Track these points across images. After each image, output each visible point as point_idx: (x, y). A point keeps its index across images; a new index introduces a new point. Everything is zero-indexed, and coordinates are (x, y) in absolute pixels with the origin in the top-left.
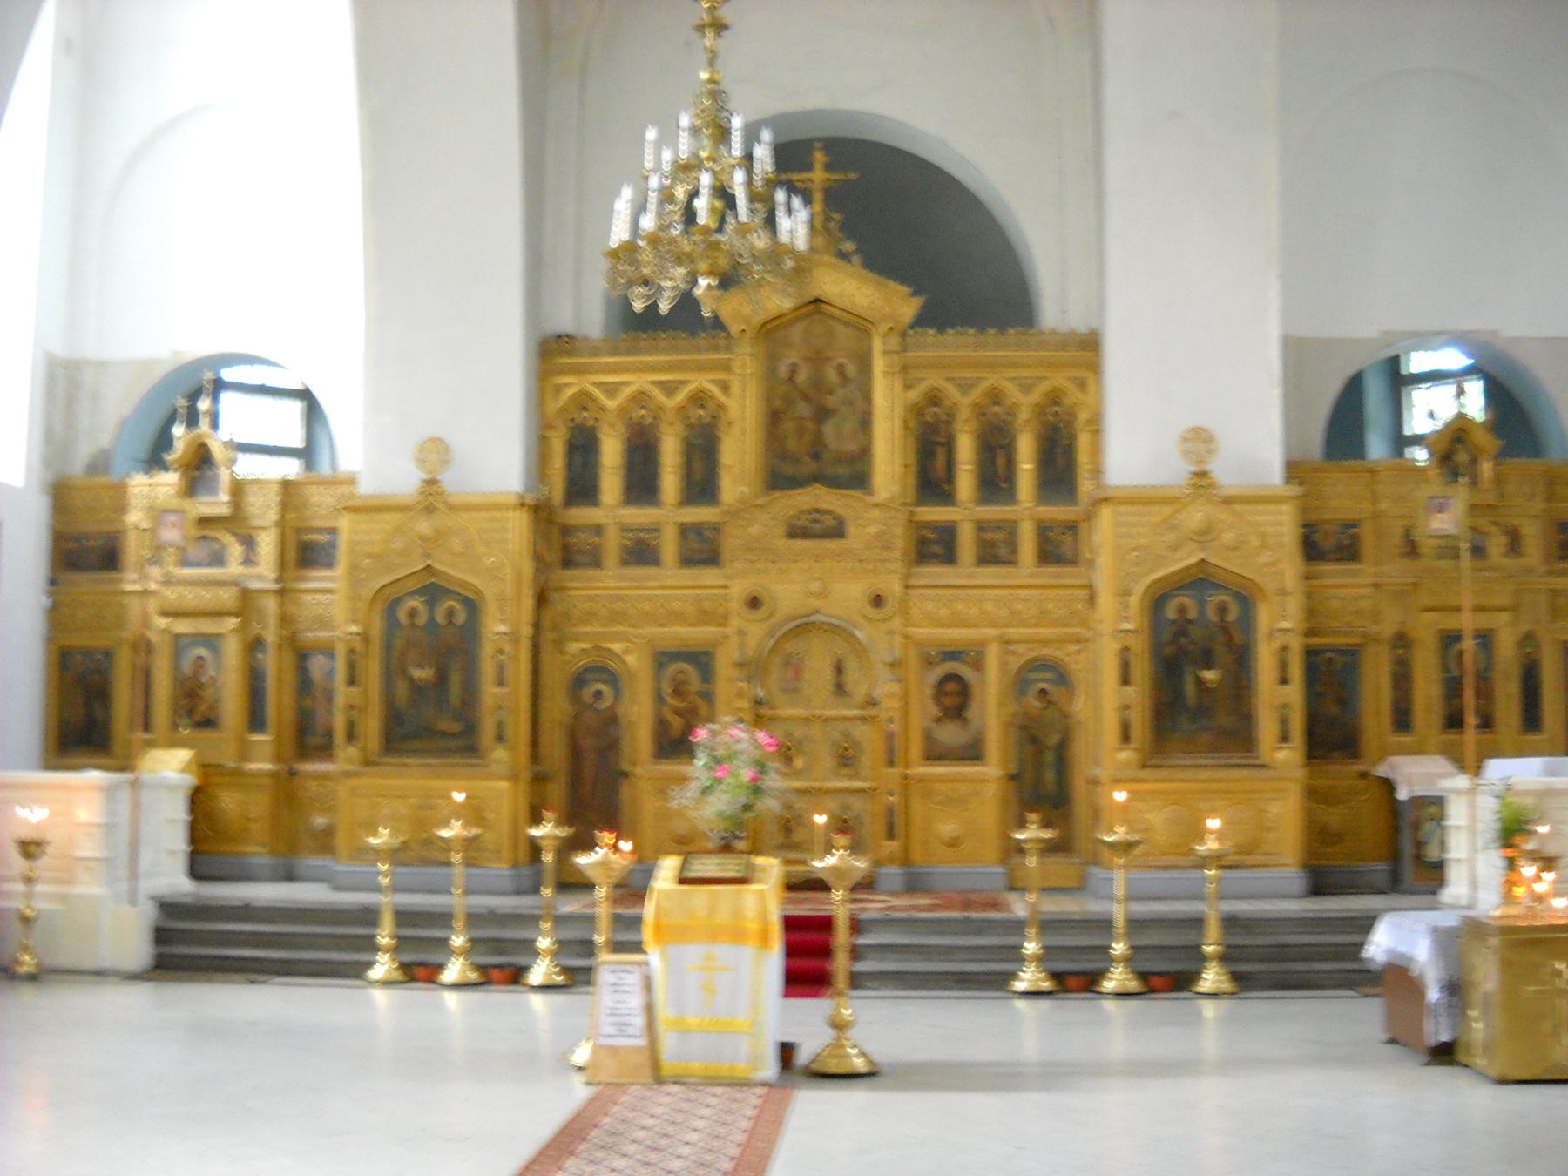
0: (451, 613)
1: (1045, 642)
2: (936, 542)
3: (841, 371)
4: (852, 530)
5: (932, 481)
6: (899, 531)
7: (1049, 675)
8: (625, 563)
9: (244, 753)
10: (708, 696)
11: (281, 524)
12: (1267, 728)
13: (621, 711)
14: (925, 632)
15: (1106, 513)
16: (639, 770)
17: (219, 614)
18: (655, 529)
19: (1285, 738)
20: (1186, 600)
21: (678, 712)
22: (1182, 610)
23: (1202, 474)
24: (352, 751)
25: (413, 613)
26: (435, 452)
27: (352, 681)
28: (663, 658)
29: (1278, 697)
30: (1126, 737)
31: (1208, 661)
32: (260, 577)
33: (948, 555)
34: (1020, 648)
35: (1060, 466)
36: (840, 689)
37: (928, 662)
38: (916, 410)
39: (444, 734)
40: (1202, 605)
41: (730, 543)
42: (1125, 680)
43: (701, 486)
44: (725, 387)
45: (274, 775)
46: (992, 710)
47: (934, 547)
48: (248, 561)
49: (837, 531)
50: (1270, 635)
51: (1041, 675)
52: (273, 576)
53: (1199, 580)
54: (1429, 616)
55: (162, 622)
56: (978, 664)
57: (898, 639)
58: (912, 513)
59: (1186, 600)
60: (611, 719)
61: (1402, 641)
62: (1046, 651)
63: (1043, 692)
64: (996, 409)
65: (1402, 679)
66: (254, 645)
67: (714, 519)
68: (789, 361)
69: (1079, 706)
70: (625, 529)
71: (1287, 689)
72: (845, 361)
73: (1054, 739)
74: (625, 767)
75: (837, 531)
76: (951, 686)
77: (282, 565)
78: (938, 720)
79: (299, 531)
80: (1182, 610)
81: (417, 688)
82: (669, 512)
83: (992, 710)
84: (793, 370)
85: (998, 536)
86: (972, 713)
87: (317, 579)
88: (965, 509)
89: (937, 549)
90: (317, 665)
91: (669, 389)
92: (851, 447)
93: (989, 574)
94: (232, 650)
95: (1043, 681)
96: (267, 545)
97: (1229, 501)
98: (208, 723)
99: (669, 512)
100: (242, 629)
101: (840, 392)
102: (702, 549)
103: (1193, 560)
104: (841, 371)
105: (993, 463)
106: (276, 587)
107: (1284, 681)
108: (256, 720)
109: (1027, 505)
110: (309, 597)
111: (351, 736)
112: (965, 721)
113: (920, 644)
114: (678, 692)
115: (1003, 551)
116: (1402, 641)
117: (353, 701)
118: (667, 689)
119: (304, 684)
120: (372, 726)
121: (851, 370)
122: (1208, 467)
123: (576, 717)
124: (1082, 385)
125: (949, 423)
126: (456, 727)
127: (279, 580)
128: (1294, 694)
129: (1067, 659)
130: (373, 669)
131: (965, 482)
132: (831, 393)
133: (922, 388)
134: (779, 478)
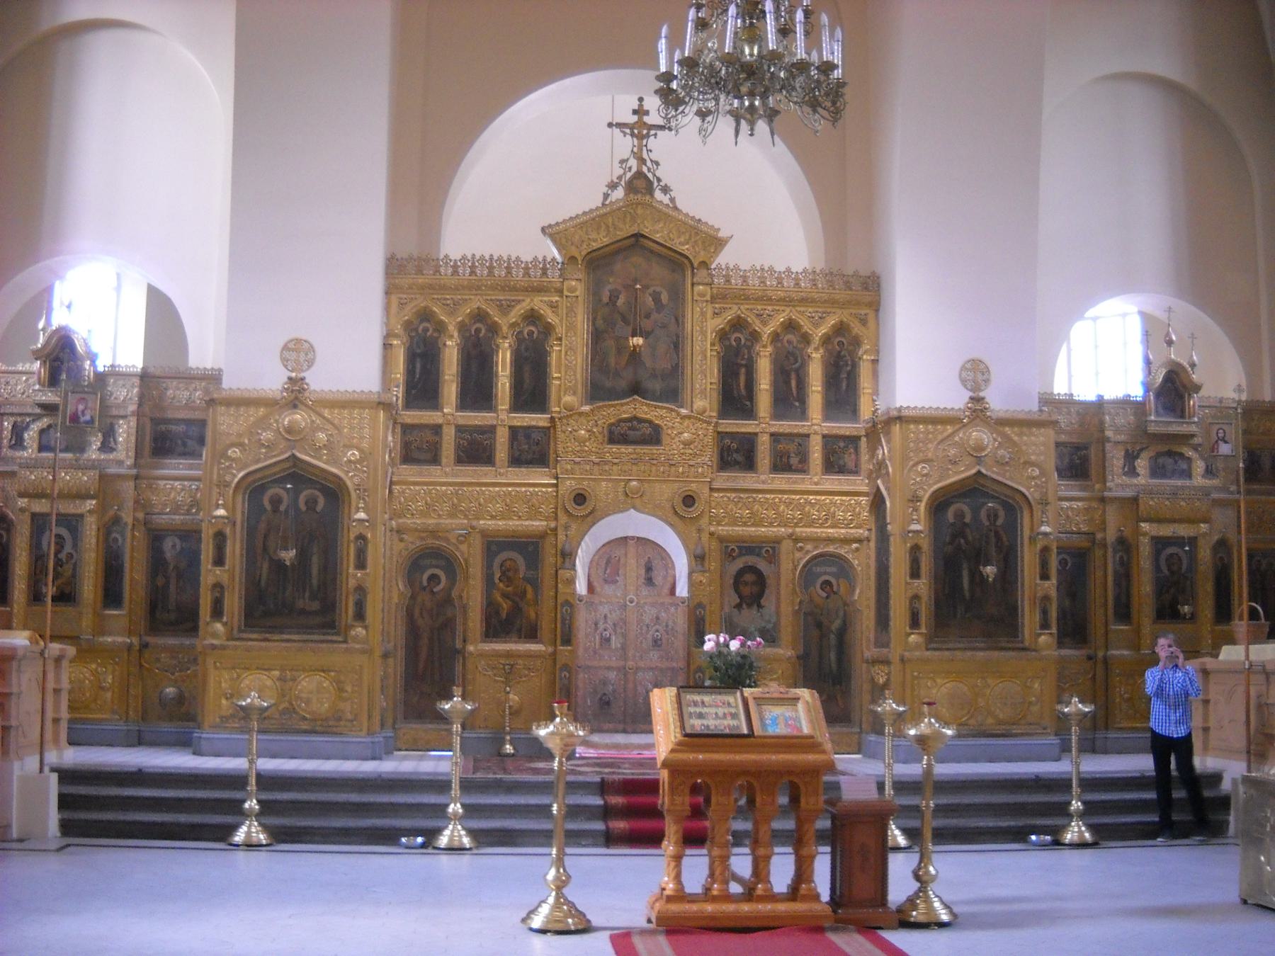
0: (311, 503)
1: (830, 540)
2: (737, 451)
3: (656, 298)
4: (665, 440)
5: (735, 399)
6: (709, 439)
7: (834, 569)
8: (459, 461)
9: (101, 630)
10: (535, 583)
11: (139, 414)
12: (1029, 619)
13: (454, 594)
14: (723, 530)
15: (896, 428)
16: (471, 648)
17: (82, 496)
18: (492, 430)
19: (1045, 625)
20: (966, 509)
21: (505, 596)
22: (960, 515)
23: (977, 400)
24: (219, 626)
25: (276, 502)
26: (297, 352)
27: (219, 561)
28: (494, 545)
29: (1036, 587)
30: (915, 622)
31: (979, 557)
32: (120, 463)
33: (749, 464)
34: (809, 547)
35: (843, 388)
36: (649, 581)
37: (729, 555)
38: (723, 336)
39: (303, 612)
40: (976, 512)
41: (564, 444)
42: (915, 574)
43: (531, 391)
44: (553, 306)
45: (130, 648)
46: (784, 602)
47: (736, 454)
48: (106, 447)
49: (654, 436)
50: (1032, 539)
51: (829, 569)
52: (129, 462)
53: (973, 489)
54: (1145, 526)
55: (22, 502)
56: (773, 557)
57: (705, 537)
58: (717, 424)
59: (966, 509)
60: (447, 601)
61: (1125, 545)
62: (831, 549)
63: (827, 583)
64: (790, 337)
65: (1125, 577)
66: (110, 527)
67: (541, 424)
68: (609, 287)
69: (863, 595)
70: (460, 429)
71: (1047, 584)
72: (658, 289)
73: (836, 624)
74: (459, 645)
75: (654, 436)
76: (749, 577)
77: (138, 454)
78: (739, 606)
79: (155, 422)
80: (960, 515)
81: (279, 566)
82: (503, 416)
83: (784, 602)
84: (614, 297)
85: (792, 447)
86: (768, 601)
87: (175, 467)
88: (764, 423)
89: (739, 457)
90: (170, 547)
91: (505, 309)
92: (664, 365)
93: (781, 481)
94: (90, 530)
95: (829, 574)
96: (125, 432)
97: (1003, 422)
98: (66, 597)
99: (503, 416)
100: (102, 509)
101: (655, 316)
102: (532, 450)
103: (974, 471)
104: (656, 298)
105: (788, 383)
106: (134, 472)
107: (1045, 576)
108: (111, 595)
109: (816, 422)
110: (162, 483)
111: (217, 612)
112: (760, 606)
113: (721, 540)
114: (507, 576)
115: (794, 461)
116: (1125, 545)
117: (222, 576)
118: (497, 575)
119: (157, 563)
120: (234, 603)
121: (665, 297)
122: (982, 394)
123: (413, 597)
124: (864, 322)
125: (750, 348)
126: (316, 606)
127: (136, 465)
128: (1051, 586)
129: (850, 557)
130: (235, 549)
131: (764, 401)
132: (648, 316)
133: (729, 316)
134: (597, 392)
